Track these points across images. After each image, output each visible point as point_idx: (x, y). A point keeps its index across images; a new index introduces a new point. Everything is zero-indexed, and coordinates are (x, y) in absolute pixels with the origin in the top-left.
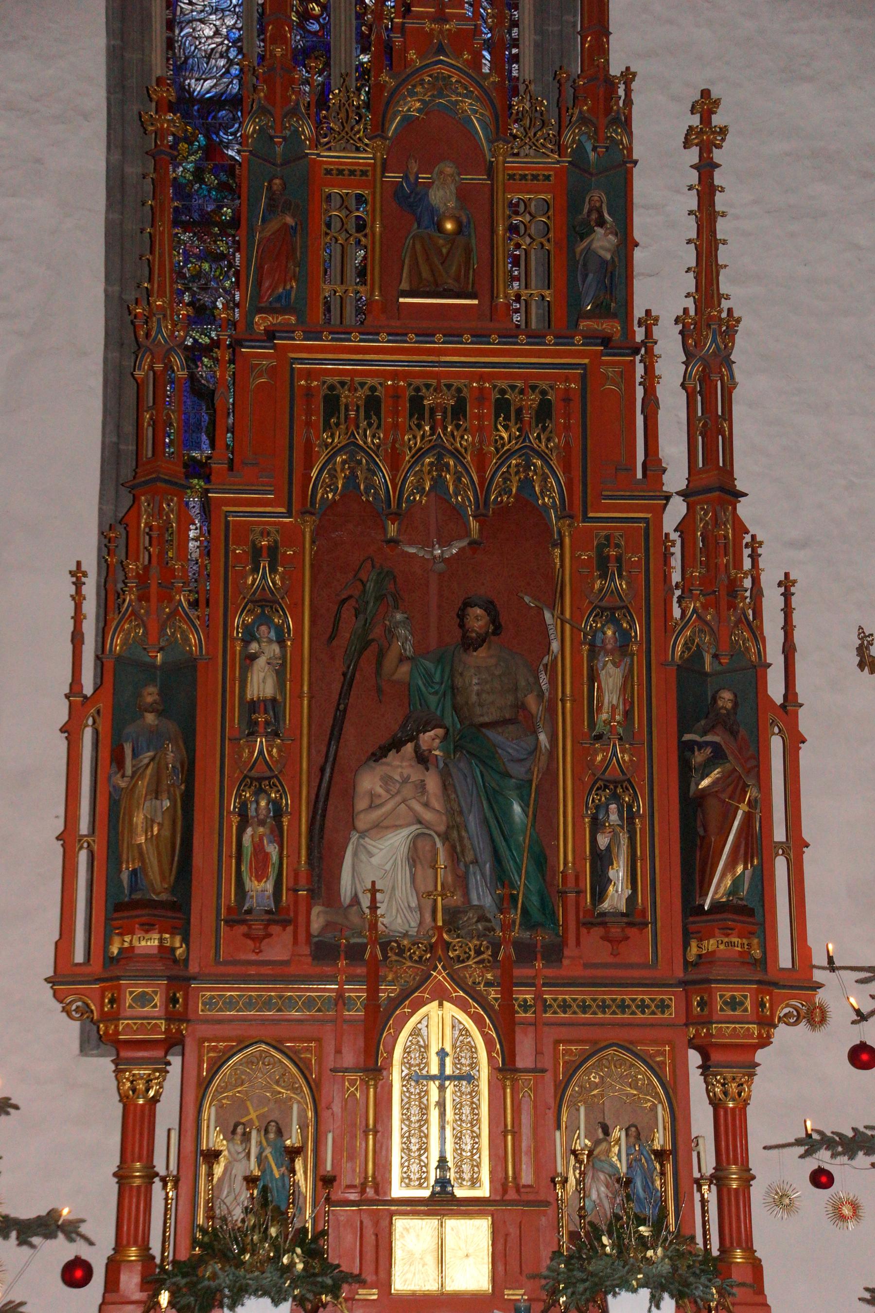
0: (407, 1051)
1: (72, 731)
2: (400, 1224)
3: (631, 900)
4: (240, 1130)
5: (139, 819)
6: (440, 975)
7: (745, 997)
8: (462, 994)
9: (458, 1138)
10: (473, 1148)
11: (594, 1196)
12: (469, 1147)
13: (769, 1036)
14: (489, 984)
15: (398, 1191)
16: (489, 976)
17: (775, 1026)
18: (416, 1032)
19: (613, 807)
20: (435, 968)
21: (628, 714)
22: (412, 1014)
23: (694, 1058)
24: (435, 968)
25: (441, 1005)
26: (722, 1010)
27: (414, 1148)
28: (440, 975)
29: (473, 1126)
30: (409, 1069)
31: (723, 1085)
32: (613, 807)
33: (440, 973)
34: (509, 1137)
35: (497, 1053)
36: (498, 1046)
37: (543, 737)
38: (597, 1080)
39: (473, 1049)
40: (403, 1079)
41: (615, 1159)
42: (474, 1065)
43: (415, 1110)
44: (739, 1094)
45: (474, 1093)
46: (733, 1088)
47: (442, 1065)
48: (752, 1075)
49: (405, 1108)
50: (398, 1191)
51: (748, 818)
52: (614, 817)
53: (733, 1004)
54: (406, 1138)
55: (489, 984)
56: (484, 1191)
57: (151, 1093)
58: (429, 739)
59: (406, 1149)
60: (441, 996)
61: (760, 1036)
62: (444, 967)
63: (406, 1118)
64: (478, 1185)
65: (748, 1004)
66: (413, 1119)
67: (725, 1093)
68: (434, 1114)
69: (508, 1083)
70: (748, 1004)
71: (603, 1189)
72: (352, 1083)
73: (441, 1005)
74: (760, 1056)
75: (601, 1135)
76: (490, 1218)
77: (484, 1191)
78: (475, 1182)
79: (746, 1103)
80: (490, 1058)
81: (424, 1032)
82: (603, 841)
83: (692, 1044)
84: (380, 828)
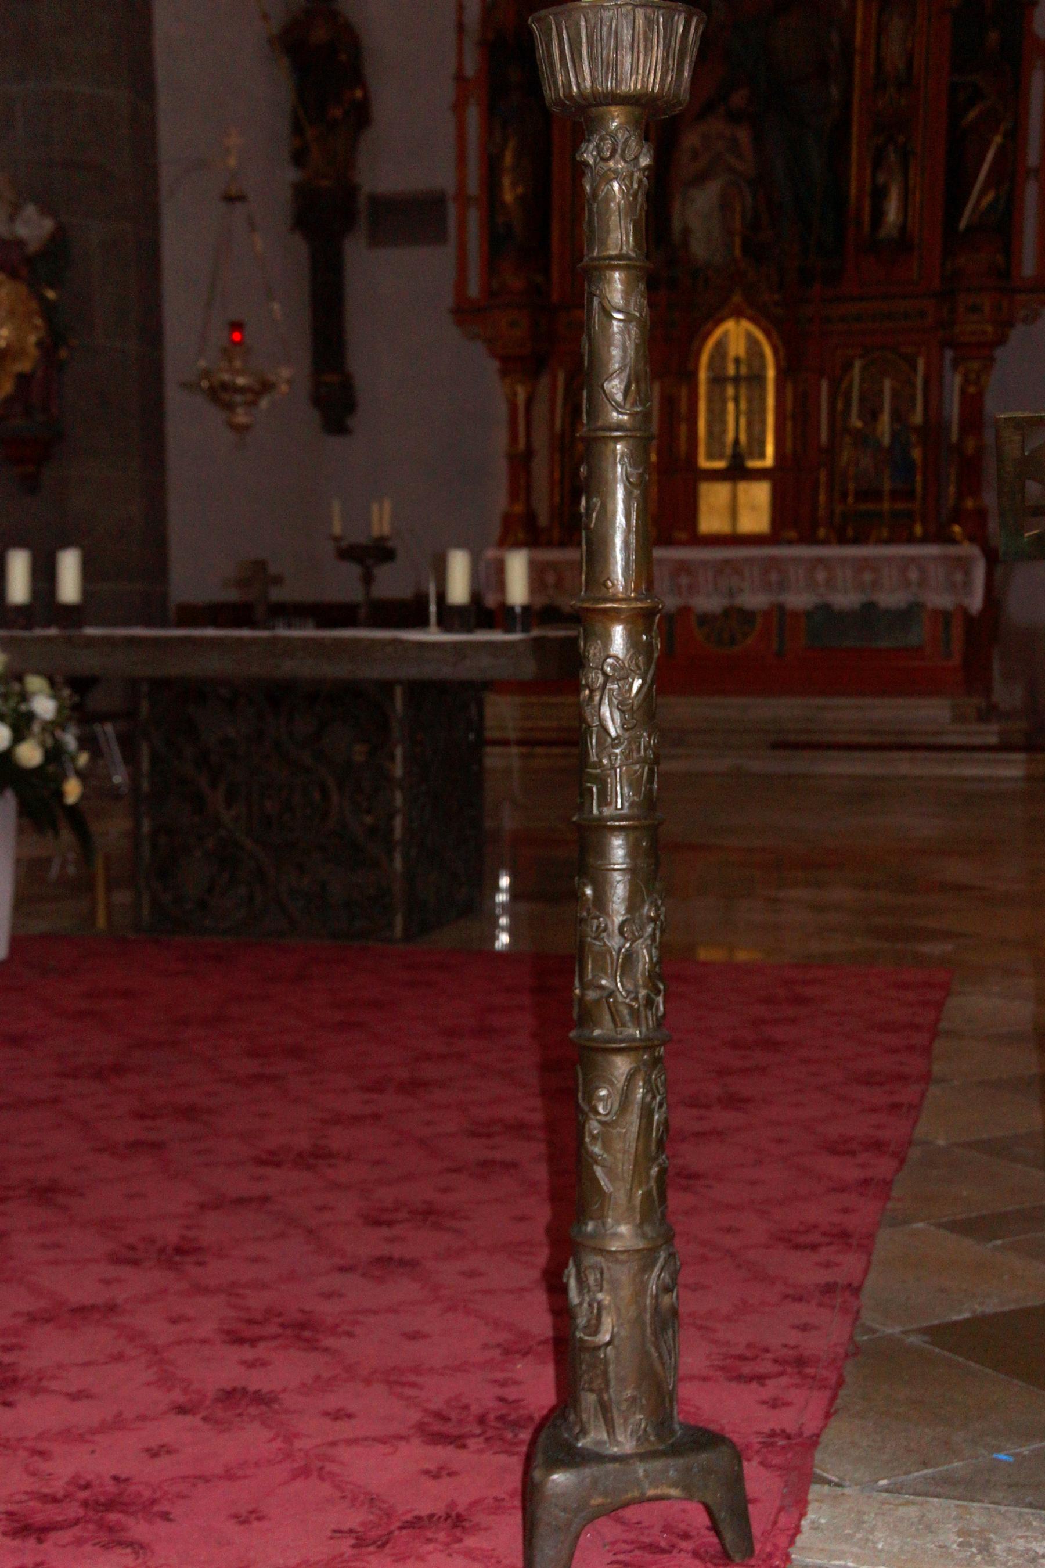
0: (712, 358)
1: (459, 107)
3: (903, 228)
5: (506, 181)
6: (737, 298)
9: (750, 424)
19: (891, 148)
21: (909, 65)
28: (737, 298)
32: (891, 148)
37: (834, 91)
39: (762, 356)
42: (763, 367)
46: (973, 376)
47: (737, 368)
49: (710, 401)
50: (704, 463)
51: (1002, 150)
52: (892, 157)
53: (975, 309)
58: (739, 98)
60: (738, 314)
63: (710, 411)
68: (731, 406)
77: (769, 461)
78: (762, 455)
82: (881, 179)
84: (701, 179)
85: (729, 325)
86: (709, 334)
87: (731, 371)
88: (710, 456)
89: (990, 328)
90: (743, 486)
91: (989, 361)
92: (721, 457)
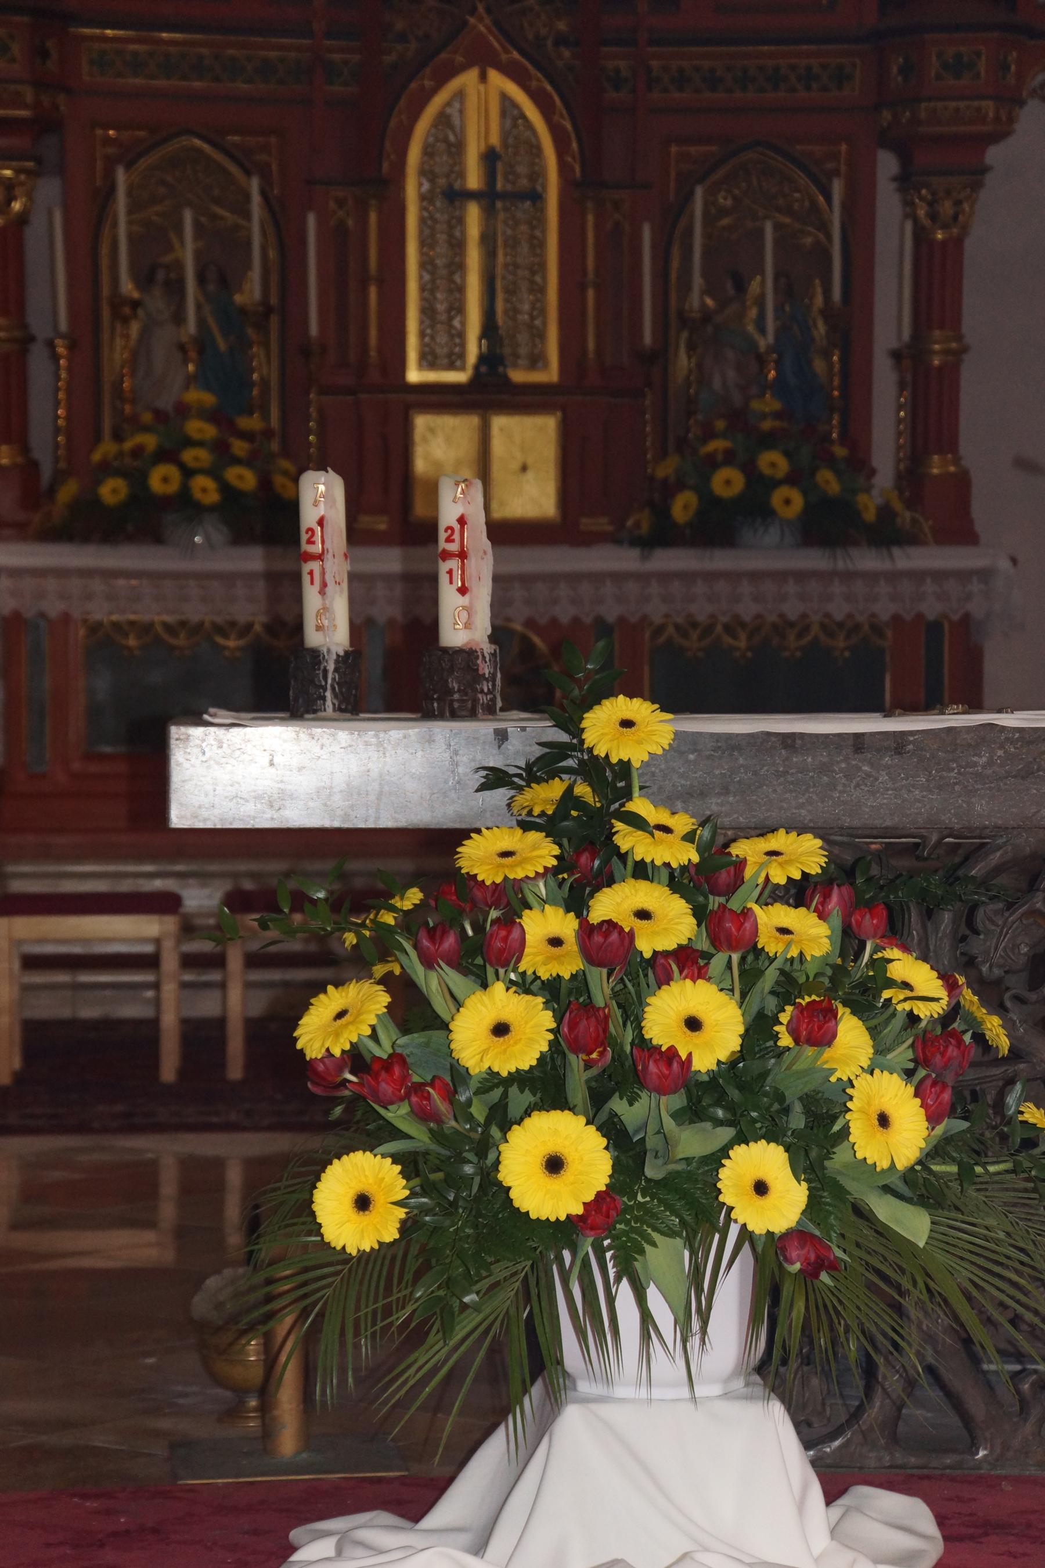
0: (428, 152)
2: (421, 422)
4: (160, 275)
7: (978, 55)
8: (516, 55)
10: (533, 308)
11: (717, 384)
12: (526, 307)
13: (1011, 120)
14: (561, 41)
15: (414, 375)
16: (562, 26)
17: (1022, 103)
18: (443, 120)
20: (473, 11)
22: (435, 91)
23: (887, 164)
24: (473, 11)
25: (483, 78)
26: (939, 77)
27: (441, 307)
28: (481, 25)
29: (533, 273)
30: (432, 181)
31: (930, 204)
33: (481, 19)
34: (591, 293)
35: (574, 158)
36: (575, 145)
38: (729, 202)
39: (536, 150)
40: (422, 198)
41: (751, 328)
43: (442, 248)
44: (955, 218)
45: (538, 220)
46: (947, 208)
48: (976, 186)
49: (426, 243)
54: (427, 290)
55: (561, 41)
56: (550, 374)
57: (17, 206)
59: (428, 311)
61: (997, 119)
62: (489, 10)
63: (426, 264)
64: (540, 364)
65: (982, 67)
66: (439, 262)
67: (933, 216)
69: (590, 205)
70: (982, 67)
71: (731, 374)
72: (341, 203)
73: (483, 78)
74: (994, 155)
75: (731, 290)
76: (559, 414)
77: (550, 374)
78: (536, 360)
79: (965, 230)
80: (562, 166)
81: (456, 122)
83: (884, 141)
85: (469, 78)
86: (427, 97)
87: (474, 181)
88: (429, 360)
89: (989, 107)
90: (500, 423)
91: (977, 174)
92: (455, 361)
